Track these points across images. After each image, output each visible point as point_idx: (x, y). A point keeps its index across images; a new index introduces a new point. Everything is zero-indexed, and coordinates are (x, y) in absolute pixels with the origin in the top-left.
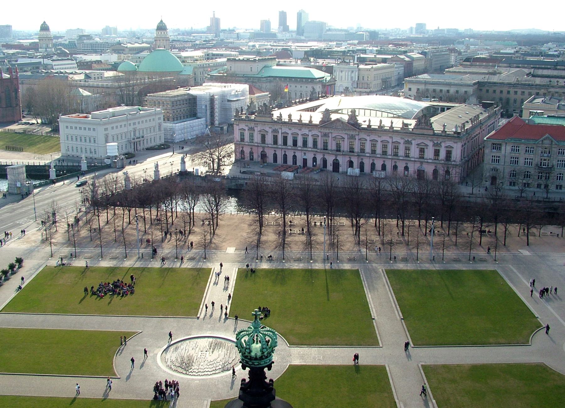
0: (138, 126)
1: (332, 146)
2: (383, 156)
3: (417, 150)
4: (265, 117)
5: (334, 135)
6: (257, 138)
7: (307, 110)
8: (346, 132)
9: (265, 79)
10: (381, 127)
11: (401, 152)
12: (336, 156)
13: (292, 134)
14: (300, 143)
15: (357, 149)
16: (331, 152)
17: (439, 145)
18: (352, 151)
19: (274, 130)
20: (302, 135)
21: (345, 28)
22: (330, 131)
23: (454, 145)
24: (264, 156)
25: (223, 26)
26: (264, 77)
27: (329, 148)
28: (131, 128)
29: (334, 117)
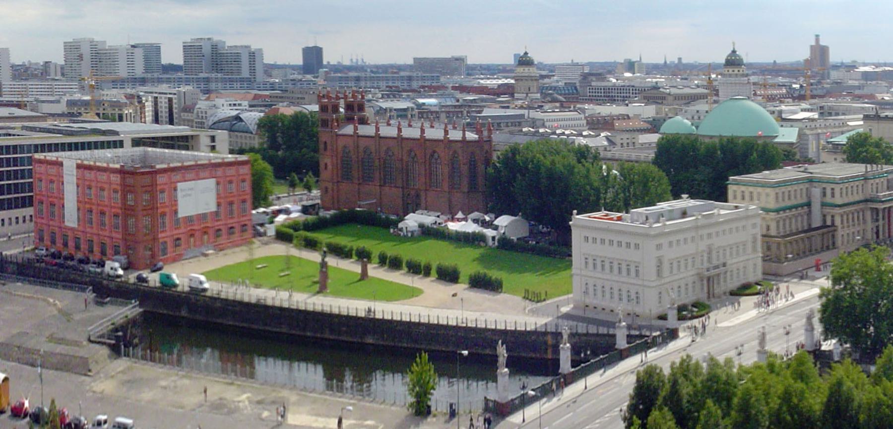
25: (834, 57)
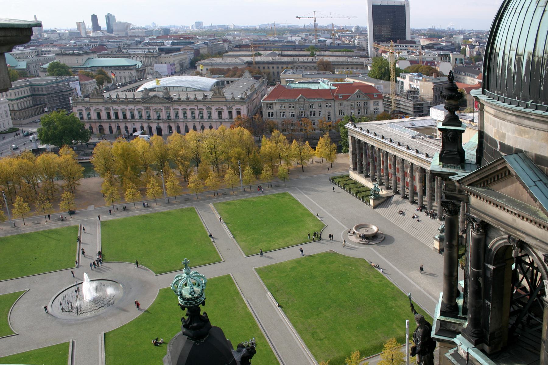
1: (153, 116)
2: (193, 120)
3: (217, 113)
4: (97, 98)
5: (154, 108)
6: (94, 116)
7: (130, 90)
9: (90, 69)
10: (188, 98)
11: (205, 116)
12: (158, 123)
13: (121, 110)
14: (129, 116)
15: (173, 116)
16: (153, 121)
17: (231, 108)
19: (106, 108)
20: (129, 110)
21: (144, 26)
22: (151, 105)
23: (242, 108)
26: (90, 67)
27: (152, 117)
29: (152, 94)
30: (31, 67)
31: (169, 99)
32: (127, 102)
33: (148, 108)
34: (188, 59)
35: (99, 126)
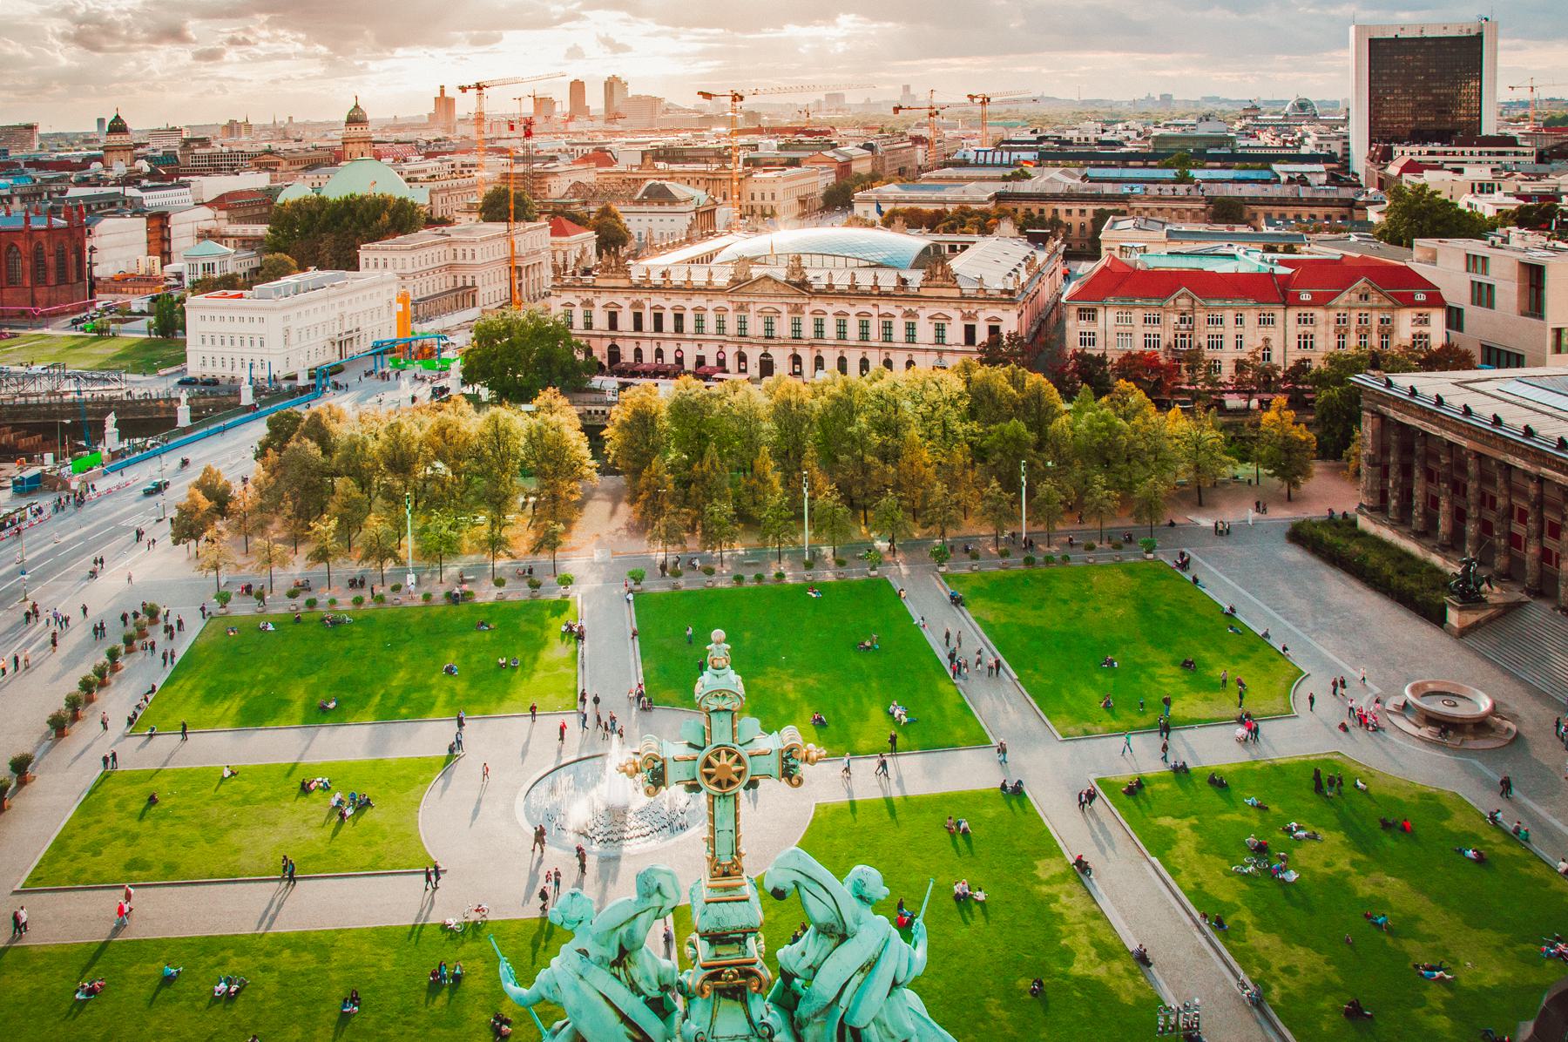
0: (349, 310)
1: (756, 327)
2: (862, 344)
3: (932, 328)
4: (616, 278)
5: (759, 307)
6: (600, 321)
8: (785, 300)
10: (853, 286)
11: (899, 333)
12: (766, 346)
15: (808, 330)
18: (797, 334)
24: (614, 353)
27: (750, 331)
28: (335, 314)
29: (756, 272)
30: (437, 198)
31: (803, 286)
32: (689, 290)
33: (741, 308)
34: (822, 185)
35: (610, 347)
